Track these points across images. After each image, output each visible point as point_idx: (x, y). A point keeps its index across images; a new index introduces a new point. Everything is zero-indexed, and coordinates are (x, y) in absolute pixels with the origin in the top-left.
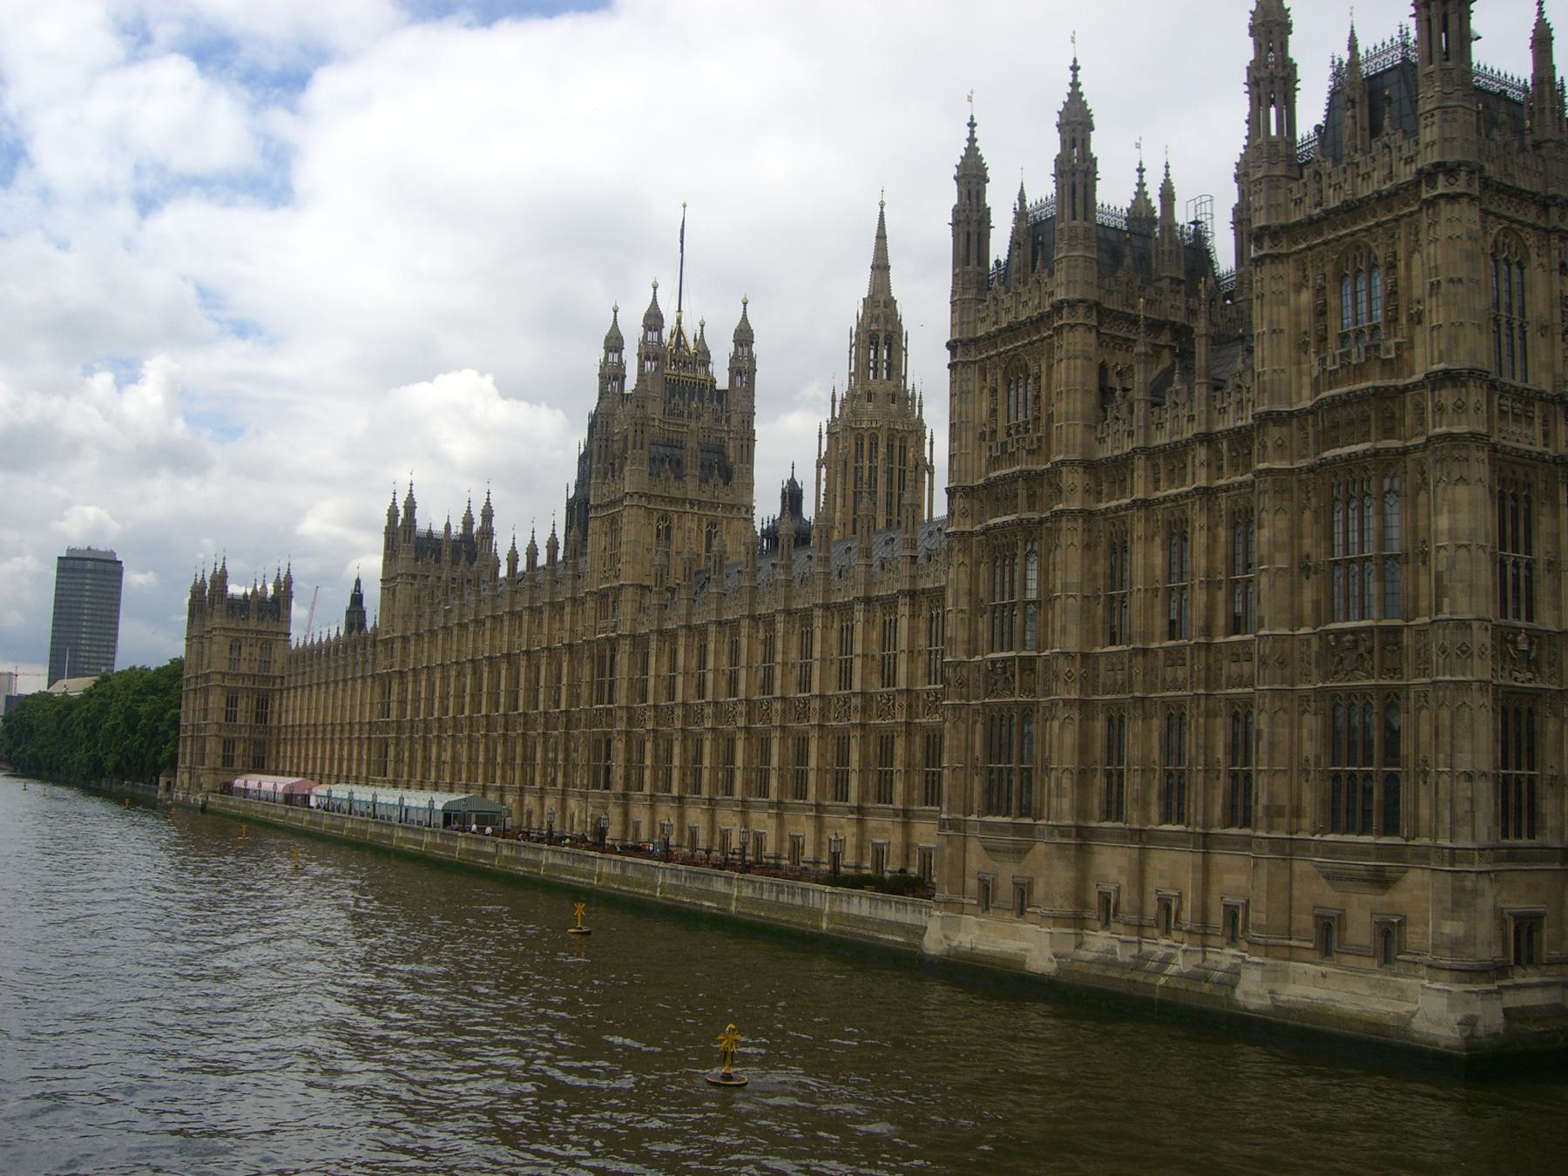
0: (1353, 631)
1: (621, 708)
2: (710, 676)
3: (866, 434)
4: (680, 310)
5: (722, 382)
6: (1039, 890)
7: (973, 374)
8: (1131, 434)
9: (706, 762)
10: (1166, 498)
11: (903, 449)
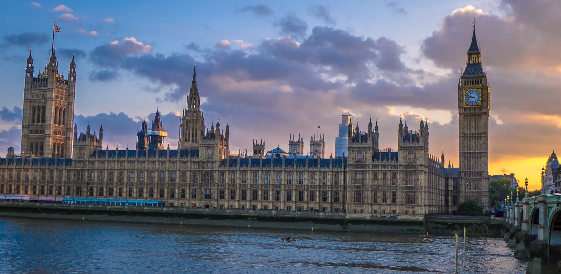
5: (66, 78)
6: (365, 210)
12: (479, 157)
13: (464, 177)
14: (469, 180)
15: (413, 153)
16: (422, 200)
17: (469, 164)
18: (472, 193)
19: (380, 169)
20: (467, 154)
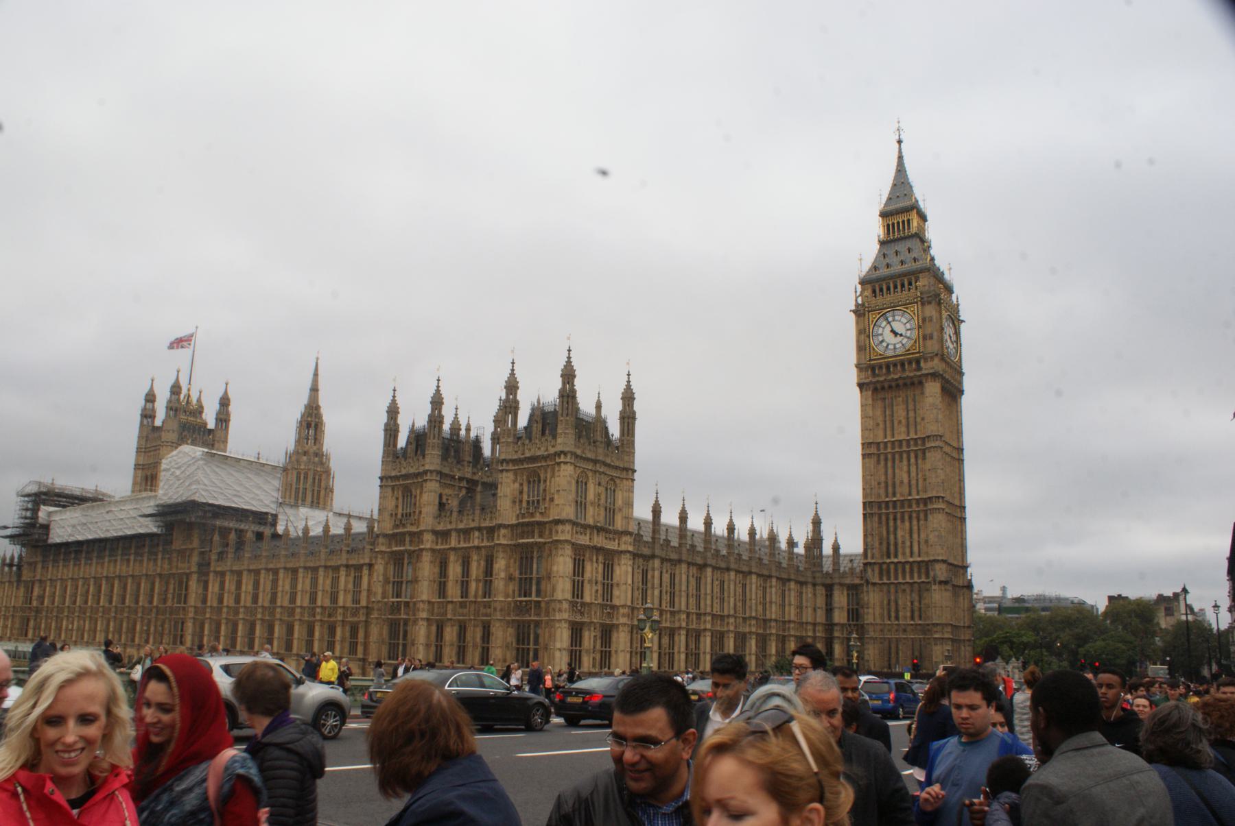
0: (526, 601)
1: (191, 606)
2: (243, 595)
3: (302, 472)
4: (190, 384)
5: (211, 425)
7: (389, 490)
8: (451, 523)
9: (239, 634)
10: (463, 548)
11: (320, 480)
12: (922, 516)
13: (876, 580)
14: (892, 589)
15: (539, 481)
16: (557, 654)
17: (892, 537)
18: (905, 631)
19: (453, 543)
20: (887, 508)
